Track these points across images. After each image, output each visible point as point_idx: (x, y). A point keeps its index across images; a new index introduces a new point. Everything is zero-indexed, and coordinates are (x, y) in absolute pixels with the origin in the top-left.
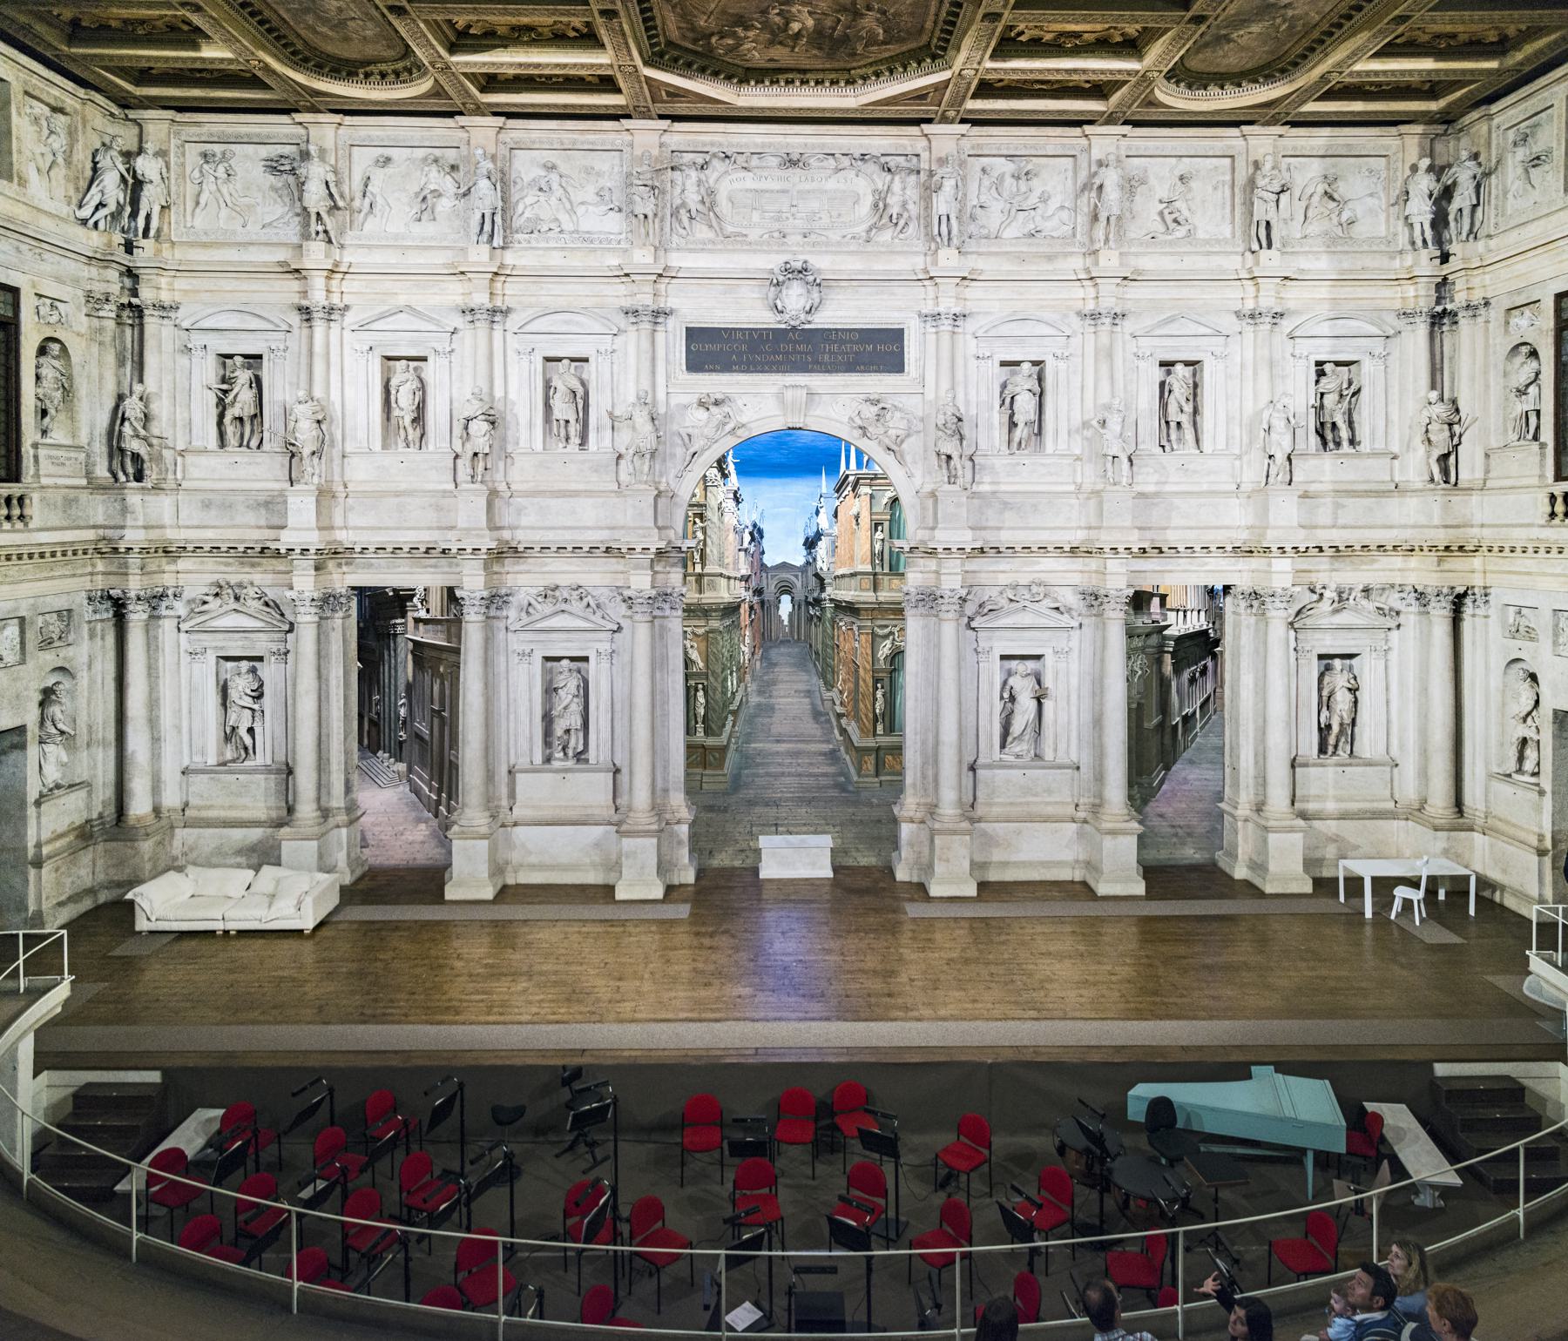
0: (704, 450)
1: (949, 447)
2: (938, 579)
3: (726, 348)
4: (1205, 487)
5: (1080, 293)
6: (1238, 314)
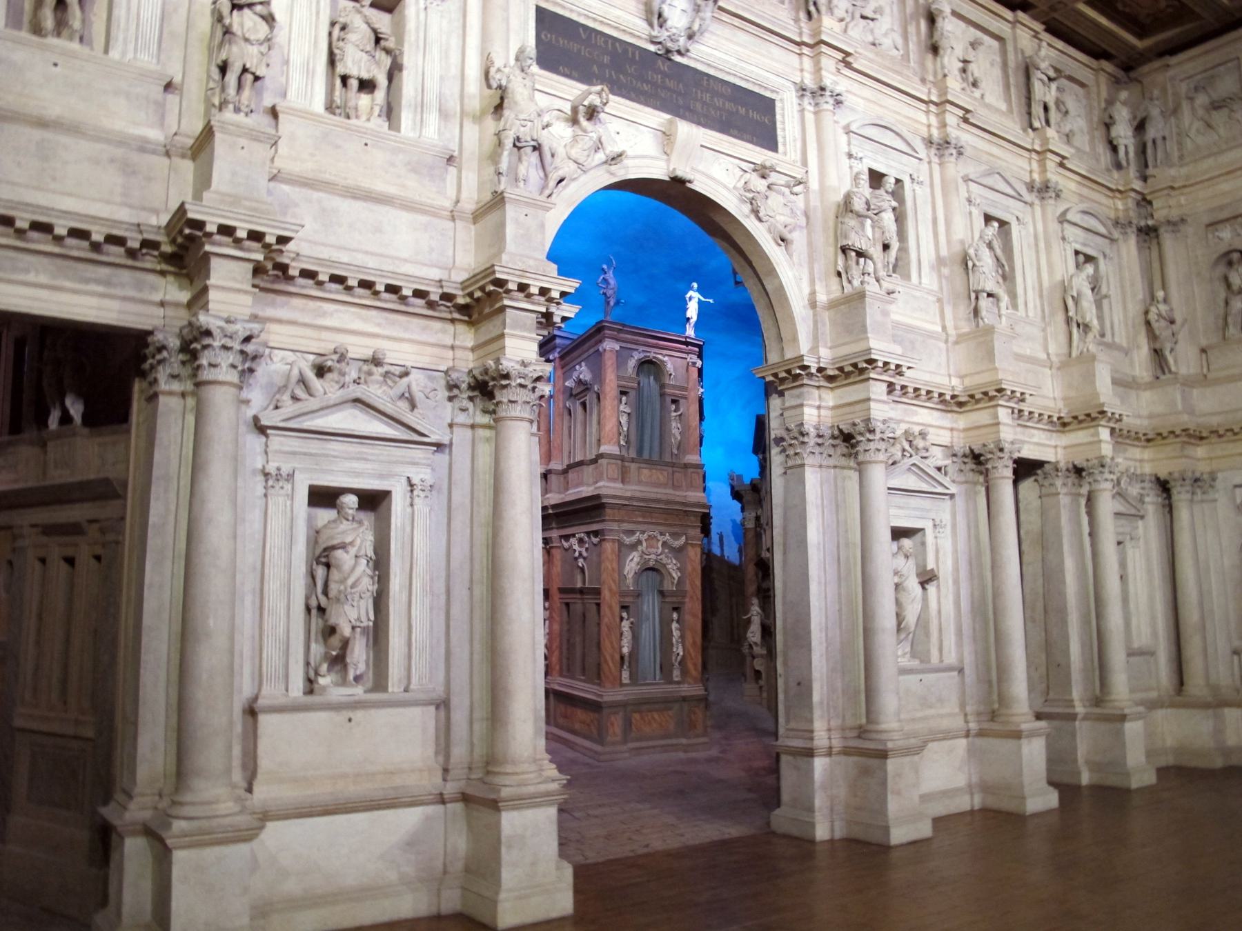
3: (585, 52)
4: (1028, 352)
5: (922, 118)
6: (1031, 187)
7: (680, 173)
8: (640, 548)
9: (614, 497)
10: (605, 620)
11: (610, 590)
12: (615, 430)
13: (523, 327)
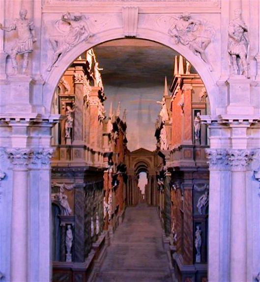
0: (66, 52)
1: (237, 49)
2: (231, 143)
7: (127, 35)
8: (206, 193)
9: (187, 167)
10: (185, 230)
11: (187, 215)
12: (190, 131)
13: (21, 133)
